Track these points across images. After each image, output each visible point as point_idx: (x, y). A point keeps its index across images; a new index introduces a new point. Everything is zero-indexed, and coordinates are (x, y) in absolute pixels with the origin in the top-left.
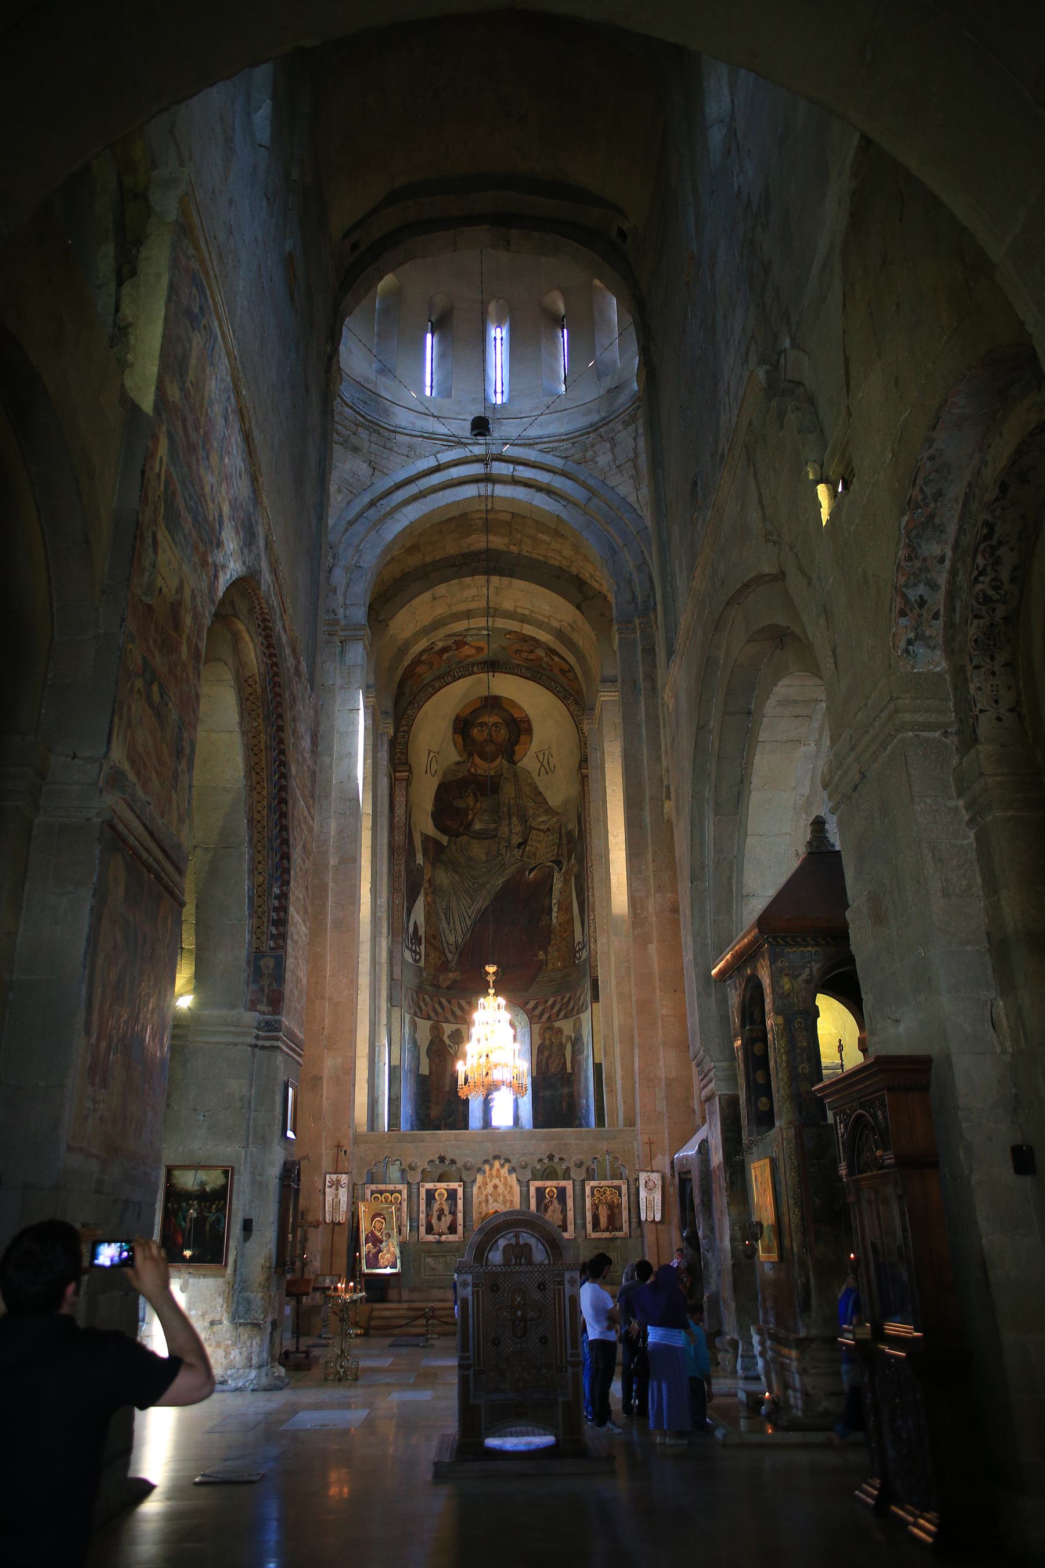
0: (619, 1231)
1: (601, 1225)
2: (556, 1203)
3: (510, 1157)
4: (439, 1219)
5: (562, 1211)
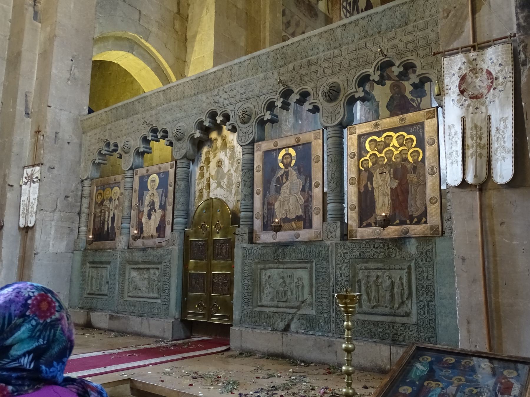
0: (418, 223)
1: (378, 212)
2: (293, 174)
3: (229, 110)
4: (149, 217)
5: (303, 190)
